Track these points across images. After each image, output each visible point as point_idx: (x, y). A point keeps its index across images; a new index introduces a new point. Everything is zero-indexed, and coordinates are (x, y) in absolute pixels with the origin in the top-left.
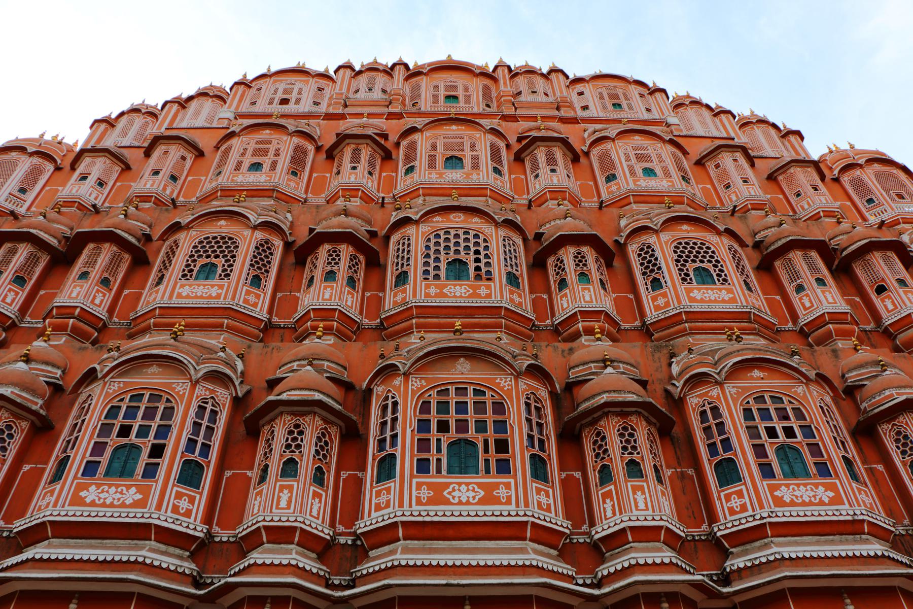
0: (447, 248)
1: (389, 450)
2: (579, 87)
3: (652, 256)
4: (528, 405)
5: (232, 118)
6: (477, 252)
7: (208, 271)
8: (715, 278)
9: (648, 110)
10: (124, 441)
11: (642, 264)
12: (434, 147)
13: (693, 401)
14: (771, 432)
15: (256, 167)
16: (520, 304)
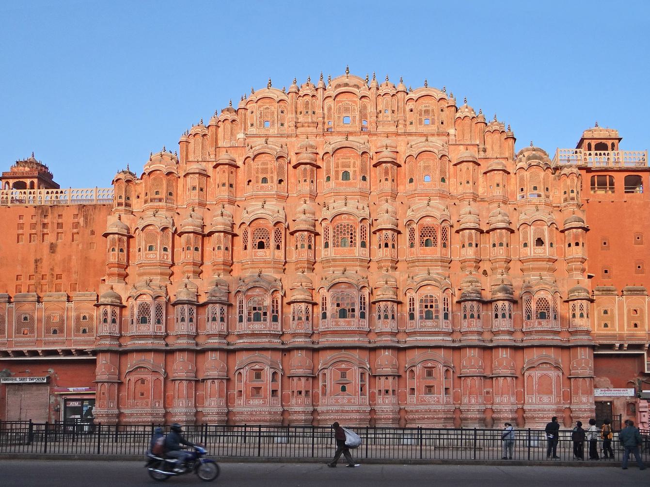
0: (341, 232)
1: (325, 311)
2: (411, 105)
3: (413, 233)
4: (361, 297)
5: (245, 137)
6: (351, 234)
7: (261, 246)
8: (433, 243)
9: (442, 123)
10: (255, 311)
11: (410, 235)
12: (338, 167)
13: (408, 294)
14: (426, 307)
15: (265, 180)
16: (365, 254)
